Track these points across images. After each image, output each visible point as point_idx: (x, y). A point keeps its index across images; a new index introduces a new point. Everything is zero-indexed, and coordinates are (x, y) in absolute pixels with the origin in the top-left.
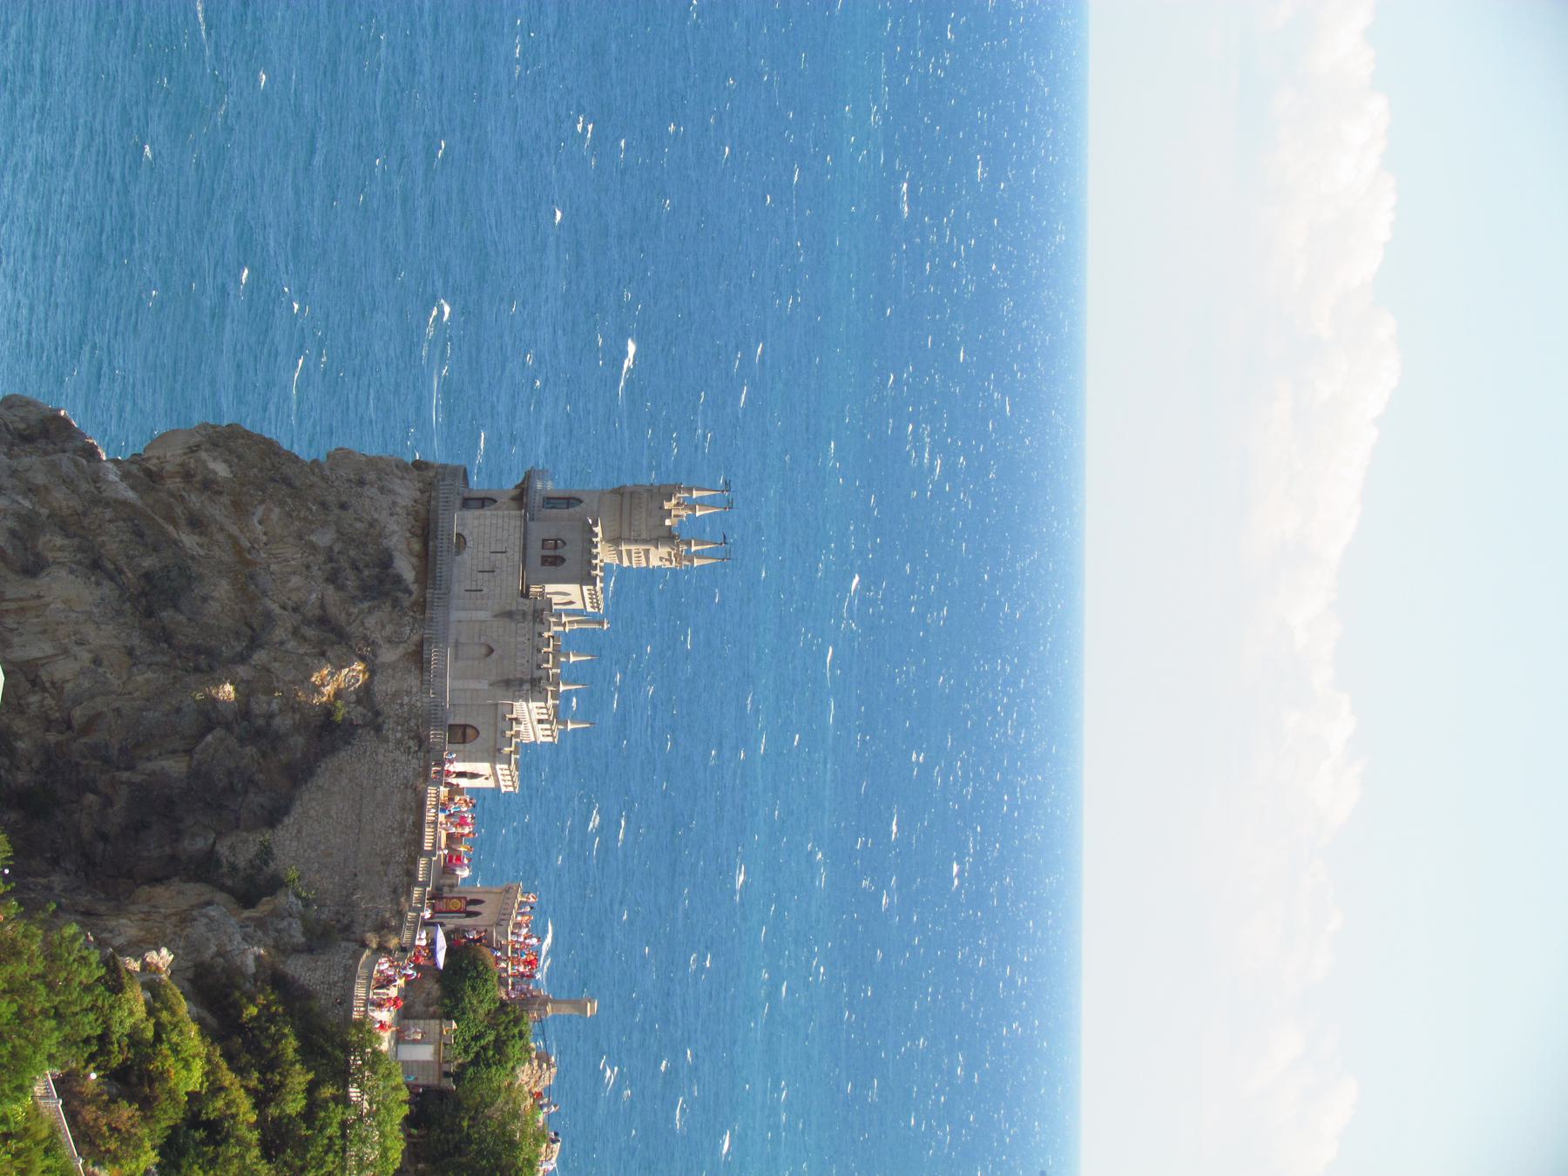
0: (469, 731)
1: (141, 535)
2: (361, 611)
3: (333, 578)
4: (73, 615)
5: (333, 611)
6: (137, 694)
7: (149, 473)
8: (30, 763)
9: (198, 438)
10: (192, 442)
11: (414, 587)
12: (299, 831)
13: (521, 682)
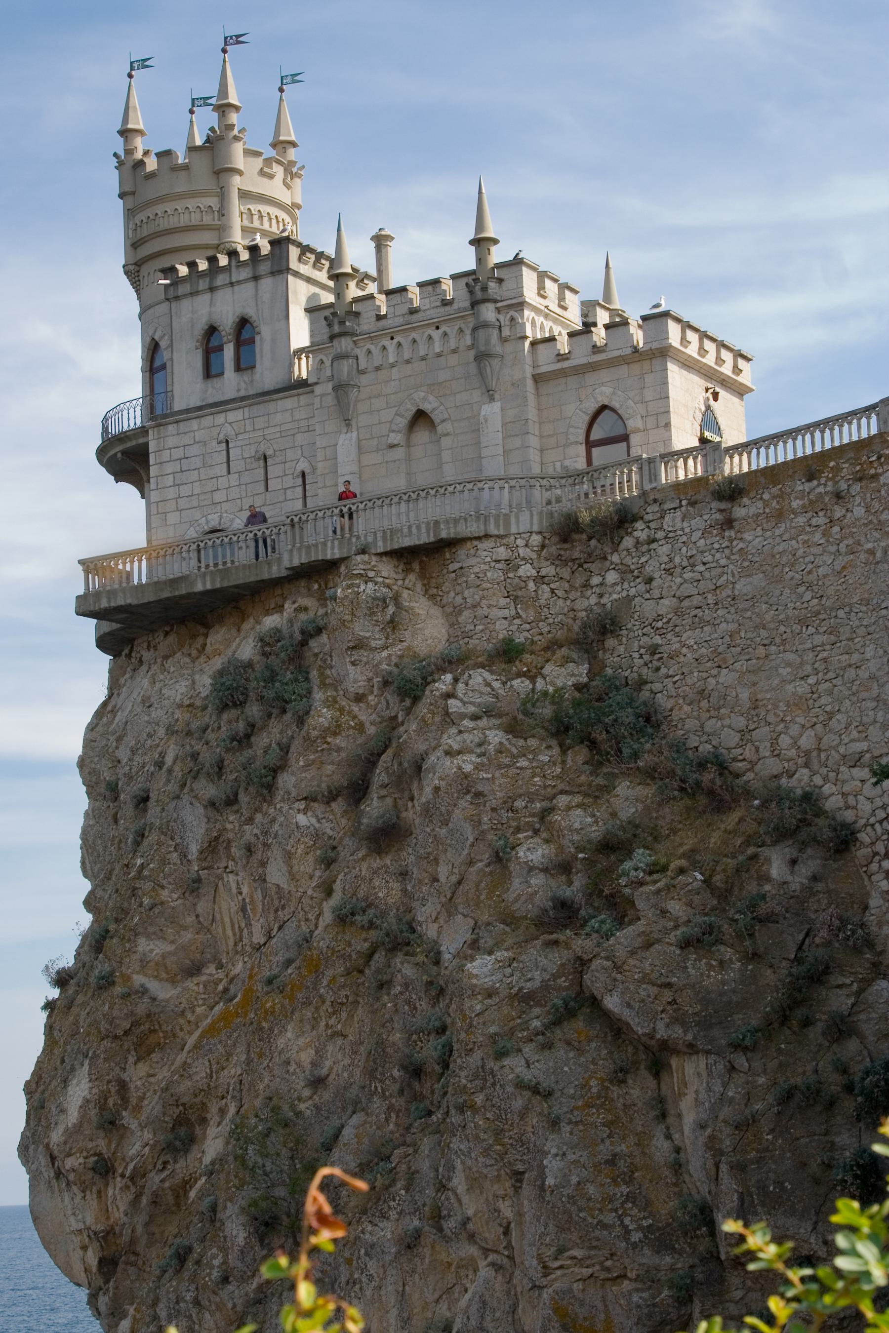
2: (331, 703)
5: (331, 773)
7: (108, 1265)
9: (43, 1160)
11: (289, 607)
13: (481, 326)
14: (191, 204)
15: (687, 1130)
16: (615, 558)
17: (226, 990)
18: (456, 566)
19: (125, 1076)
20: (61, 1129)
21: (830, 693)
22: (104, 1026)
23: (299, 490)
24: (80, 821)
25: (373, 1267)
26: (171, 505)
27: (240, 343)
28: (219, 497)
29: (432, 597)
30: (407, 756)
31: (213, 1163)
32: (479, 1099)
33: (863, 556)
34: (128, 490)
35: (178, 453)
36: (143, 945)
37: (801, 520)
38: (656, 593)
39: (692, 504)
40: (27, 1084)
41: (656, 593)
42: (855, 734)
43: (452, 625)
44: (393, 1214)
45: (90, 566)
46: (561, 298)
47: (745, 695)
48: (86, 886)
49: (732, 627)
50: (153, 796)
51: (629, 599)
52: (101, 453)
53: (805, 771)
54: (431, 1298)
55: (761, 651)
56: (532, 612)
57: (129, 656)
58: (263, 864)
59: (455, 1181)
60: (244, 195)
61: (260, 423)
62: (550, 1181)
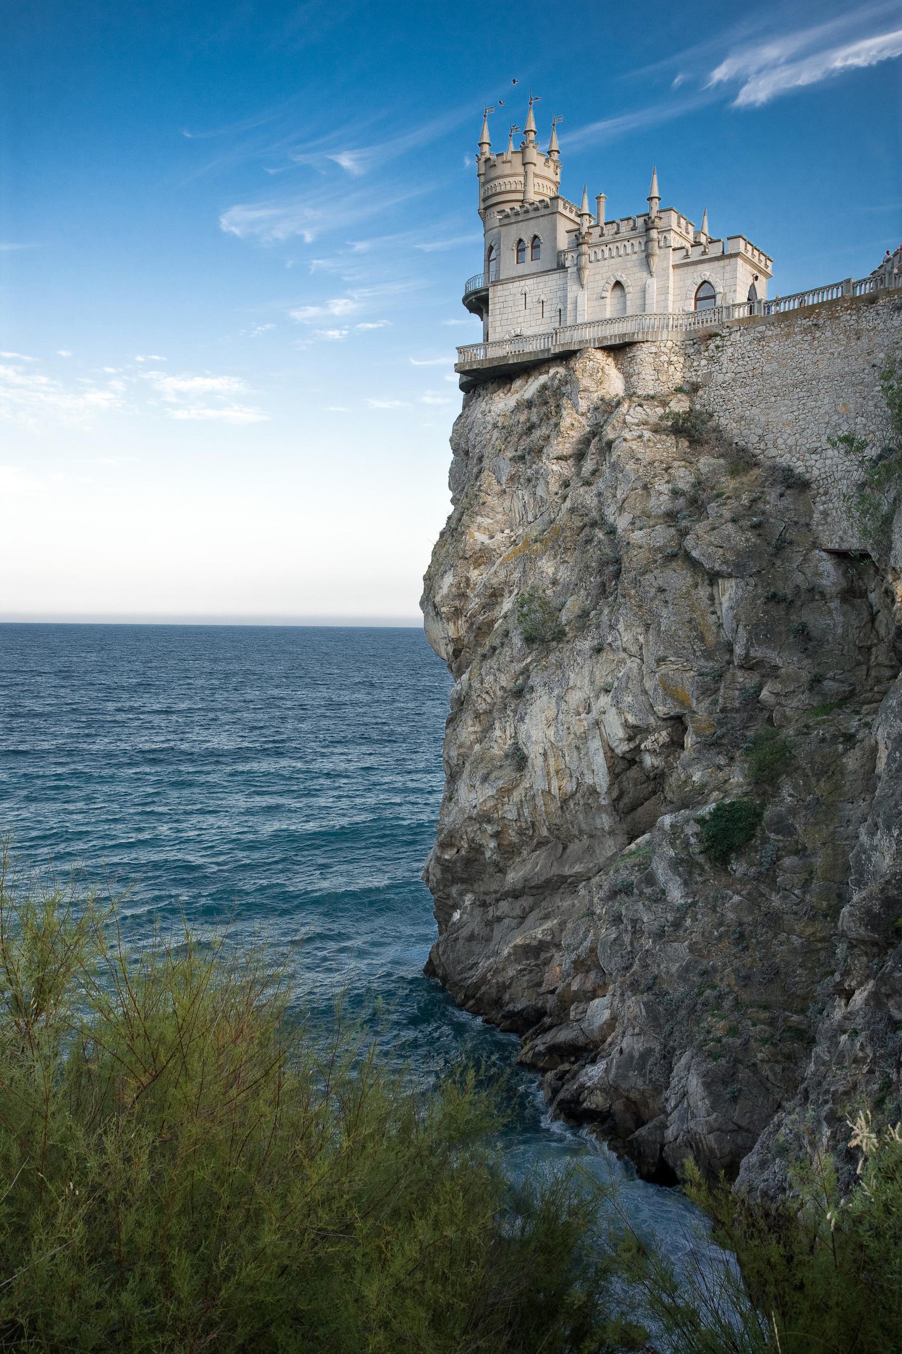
0: (701, 295)
1: (494, 649)
3: (538, 451)
4: (561, 716)
6: (641, 639)
8: (719, 768)
9: (430, 608)
10: (433, 614)
11: (552, 371)
12: (815, 451)
14: (512, 179)
15: (724, 610)
16: (706, 354)
17: (515, 541)
18: (631, 355)
19: (468, 575)
20: (440, 595)
21: (804, 419)
22: (461, 553)
23: (558, 318)
24: (449, 466)
25: (579, 659)
26: (498, 323)
27: (533, 248)
28: (520, 320)
29: (619, 369)
30: (605, 440)
31: (506, 613)
32: (633, 592)
33: (828, 355)
34: (476, 317)
35: (502, 299)
36: (479, 519)
37: (799, 338)
38: (724, 370)
39: (746, 329)
40: (424, 576)
41: (724, 370)
42: (815, 439)
43: (627, 382)
44: (589, 638)
45: (461, 350)
46: (687, 229)
47: (763, 419)
48: (450, 494)
49: (759, 387)
50: (486, 455)
51: (711, 373)
52: (464, 300)
53: (788, 455)
54: (604, 674)
55: (773, 399)
56: (665, 377)
57: (474, 392)
58: (535, 487)
59: (619, 626)
60: (536, 176)
61: (541, 285)
62: (663, 629)
